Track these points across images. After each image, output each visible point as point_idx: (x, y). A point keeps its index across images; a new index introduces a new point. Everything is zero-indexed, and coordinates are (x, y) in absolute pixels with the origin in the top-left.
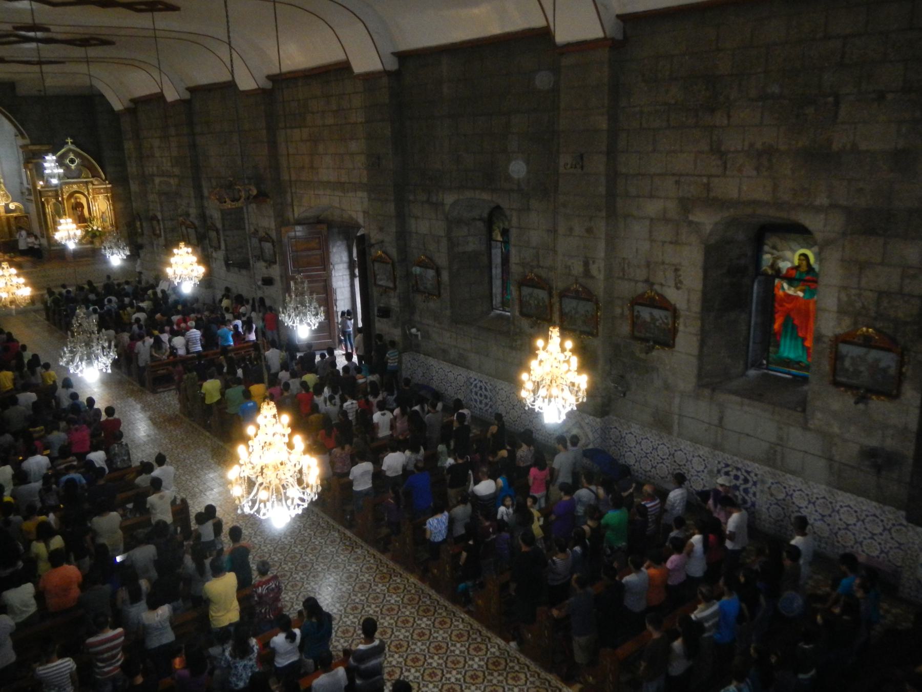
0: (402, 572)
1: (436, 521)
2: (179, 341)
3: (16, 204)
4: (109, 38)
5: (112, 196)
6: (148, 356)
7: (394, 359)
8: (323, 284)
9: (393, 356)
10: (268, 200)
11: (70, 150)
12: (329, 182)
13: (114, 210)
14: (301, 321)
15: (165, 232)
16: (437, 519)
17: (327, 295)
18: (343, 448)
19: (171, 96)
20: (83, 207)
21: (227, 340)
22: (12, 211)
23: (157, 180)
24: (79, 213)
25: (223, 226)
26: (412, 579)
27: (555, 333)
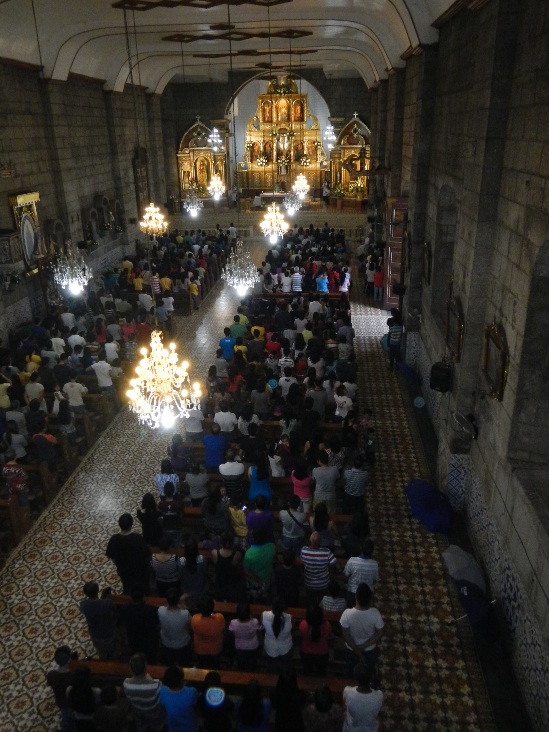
2: (286, 280)
4: (308, 29)
7: (396, 335)
9: (395, 332)
11: (355, 122)
18: (223, 395)
21: (321, 287)
27: (156, 338)
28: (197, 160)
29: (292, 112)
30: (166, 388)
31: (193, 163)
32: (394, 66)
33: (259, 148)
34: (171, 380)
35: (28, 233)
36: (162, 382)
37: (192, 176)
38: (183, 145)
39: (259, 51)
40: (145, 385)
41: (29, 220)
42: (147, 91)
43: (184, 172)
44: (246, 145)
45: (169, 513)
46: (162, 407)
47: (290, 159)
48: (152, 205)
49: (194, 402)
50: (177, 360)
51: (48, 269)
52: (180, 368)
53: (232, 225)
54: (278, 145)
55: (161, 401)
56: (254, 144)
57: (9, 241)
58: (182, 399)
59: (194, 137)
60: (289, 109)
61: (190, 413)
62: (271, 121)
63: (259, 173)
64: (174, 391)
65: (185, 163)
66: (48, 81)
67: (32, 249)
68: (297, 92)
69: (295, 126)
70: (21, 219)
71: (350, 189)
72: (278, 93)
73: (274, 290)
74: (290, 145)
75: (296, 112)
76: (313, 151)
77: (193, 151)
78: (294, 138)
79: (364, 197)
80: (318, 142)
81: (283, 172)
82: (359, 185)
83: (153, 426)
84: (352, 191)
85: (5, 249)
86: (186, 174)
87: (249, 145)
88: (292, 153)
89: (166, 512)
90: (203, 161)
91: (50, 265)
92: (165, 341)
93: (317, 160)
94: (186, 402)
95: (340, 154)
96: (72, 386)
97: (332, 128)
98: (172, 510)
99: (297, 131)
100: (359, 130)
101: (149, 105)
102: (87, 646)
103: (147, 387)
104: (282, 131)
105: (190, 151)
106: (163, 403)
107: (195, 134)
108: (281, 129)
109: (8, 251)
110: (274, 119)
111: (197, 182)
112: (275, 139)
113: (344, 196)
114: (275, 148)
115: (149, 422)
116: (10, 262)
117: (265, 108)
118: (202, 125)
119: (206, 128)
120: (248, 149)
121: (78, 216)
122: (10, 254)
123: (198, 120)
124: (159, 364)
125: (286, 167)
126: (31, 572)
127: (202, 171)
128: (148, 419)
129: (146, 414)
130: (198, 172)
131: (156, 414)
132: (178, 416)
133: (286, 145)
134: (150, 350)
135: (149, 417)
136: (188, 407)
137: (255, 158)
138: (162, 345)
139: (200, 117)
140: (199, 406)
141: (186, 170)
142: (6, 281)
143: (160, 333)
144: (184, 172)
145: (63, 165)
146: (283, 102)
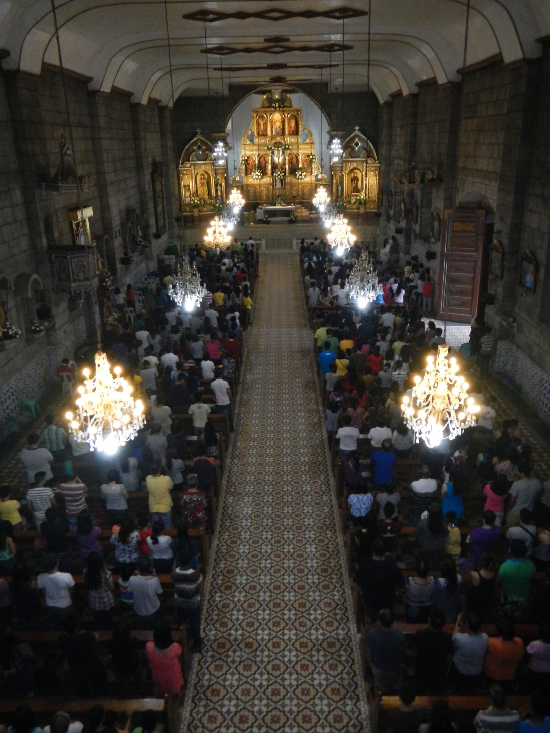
0: (338, 530)
1: (356, 499)
3: (324, 175)
5: (379, 173)
6: (316, 300)
8: (473, 264)
10: (442, 184)
11: (356, 136)
12: (482, 171)
13: (379, 184)
14: (364, 294)
15: (395, 205)
16: (358, 498)
17: (474, 275)
19: (405, 92)
20: (358, 180)
22: (321, 180)
23: (396, 162)
24: (354, 185)
25: (422, 204)
26: (340, 540)
29: (287, 126)
32: (450, 80)
33: (254, 161)
37: (193, 189)
39: (289, 65)
42: (160, 104)
43: (185, 186)
45: (388, 535)
47: (285, 172)
51: (105, 286)
53: (251, 238)
54: (272, 159)
56: (248, 158)
60: (283, 122)
62: (265, 135)
63: (254, 186)
65: (186, 177)
66: (95, 93)
68: (291, 106)
69: (289, 139)
71: (353, 201)
72: (273, 107)
73: (331, 302)
74: (284, 159)
75: (289, 126)
76: (308, 164)
77: (194, 164)
78: (288, 151)
79: (366, 209)
80: (313, 156)
81: (279, 185)
82: (362, 197)
84: (355, 202)
85: (84, 266)
86: (187, 188)
88: (287, 167)
89: (385, 533)
90: (203, 175)
91: (106, 282)
93: (312, 173)
95: (342, 167)
96: (199, 408)
97: (339, 141)
98: (391, 531)
99: (292, 144)
100: (360, 144)
101: (162, 119)
102: (342, 679)
104: (278, 145)
105: (191, 164)
107: (195, 148)
108: (276, 143)
110: (269, 133)
111: (197, 196)
112: (269, 152)
113: (346, 208)
114: (270, 162)
116: (87, 279)
117: (260, 121)
118: (202, 138)
119: (207, 141)
125: (281, 180)
127: (202, 185)
130: (199, 186)
133: (281, 159)
137: (249, 172)
141: (187, 184)
142: (81, 299)
145: (110, 177)
146: (277, 116)
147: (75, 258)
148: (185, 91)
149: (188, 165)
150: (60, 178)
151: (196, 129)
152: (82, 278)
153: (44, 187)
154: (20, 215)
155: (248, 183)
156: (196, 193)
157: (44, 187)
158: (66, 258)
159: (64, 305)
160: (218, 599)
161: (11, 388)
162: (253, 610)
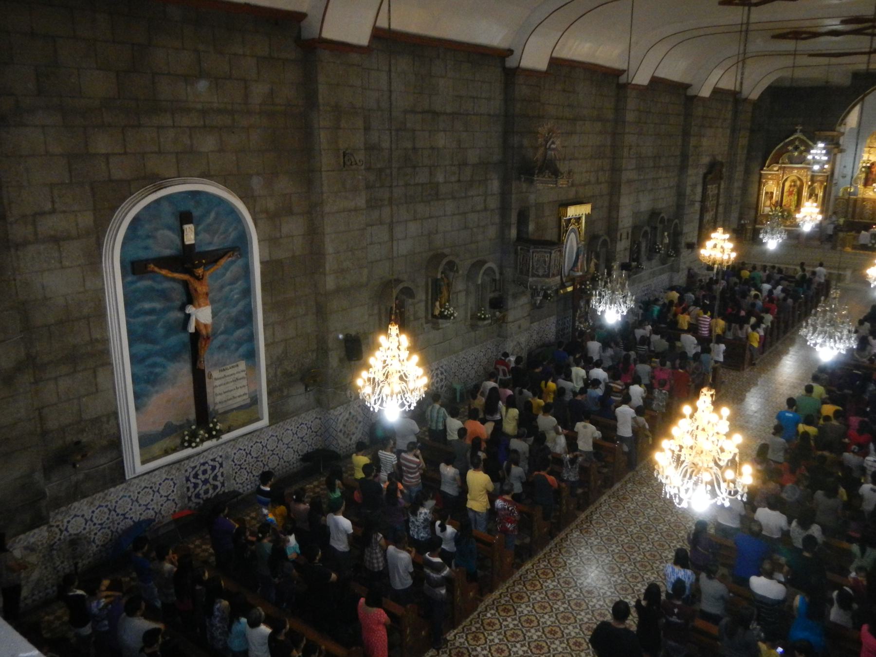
28: (786, 180)
30: (706, 461)
31: (781, 182)
34: (715, 454)
35: (572, 246)
36: (702, 452)
38: (771, 161)
40: (680, 451)
41: (575, 233)
43: (767, 193)
44: (861, 165)
45: (674, 619)
46: (696, 483)
48: (720, 230)
49: (740, 490)
50: (727, 430)
52: (729, 441)
53: (821, 265)
55: (696, 476)
56: (873, 164)
57: (551, 253)
58: (725, 481)
59: (788, 151)
61: (731, 501)
64: (715, 468)
65: (771, 182)
66: (626, 86)
67: (571, 265)
70: (567, 231)
77: (785, 167)
83: (679, 504)
85: (545, 262)
86: (769, 195)
87: (864, 165)
90: (794, 181)
91: (586, 285)
92: (717, 403)
94: (728, 486)
96: (585, 427)
98: (678, 615)
101: (736, 113)
103: (682, 453)
105: (780, 168)
106: (698, 479)
107: (790, 148)
109: (547, 264)
111: (781, 206)
115: (675, 497)
116: (548, 276)
120: (863, 169)
121: (628, 234)
122: (549, 268)
123: (798, 131)
124: (703, 430)
126: (501, 628)
127: (791, 193)
128: (675, 494)
129: (674, 487)
130: (785, 194)
131: (687, 490)
132: (714, 501)
134: (695, 409)
135: (677, 492)
136: (730, 493)
137: (870, 182)
138: (712, 407)
139: (801, 128)
140: (745, 495)
141: (769, 191)
142: (538, 295)
143: (713, 392)
144: (767, 193)
147: (537, 252)
148: (777, 80)
149: (776, 169)
150: (537, 171)
151: (797, 125)
152: (540, 274)
153: (523, 180)
154: (494, 203)
155: (866, 196)
156: (780, 203)
157: (523, 180)
158: (529, 251)
159: (524, 300)
160: (489, 615)
161: (442, 367)
162: (513, 639)
